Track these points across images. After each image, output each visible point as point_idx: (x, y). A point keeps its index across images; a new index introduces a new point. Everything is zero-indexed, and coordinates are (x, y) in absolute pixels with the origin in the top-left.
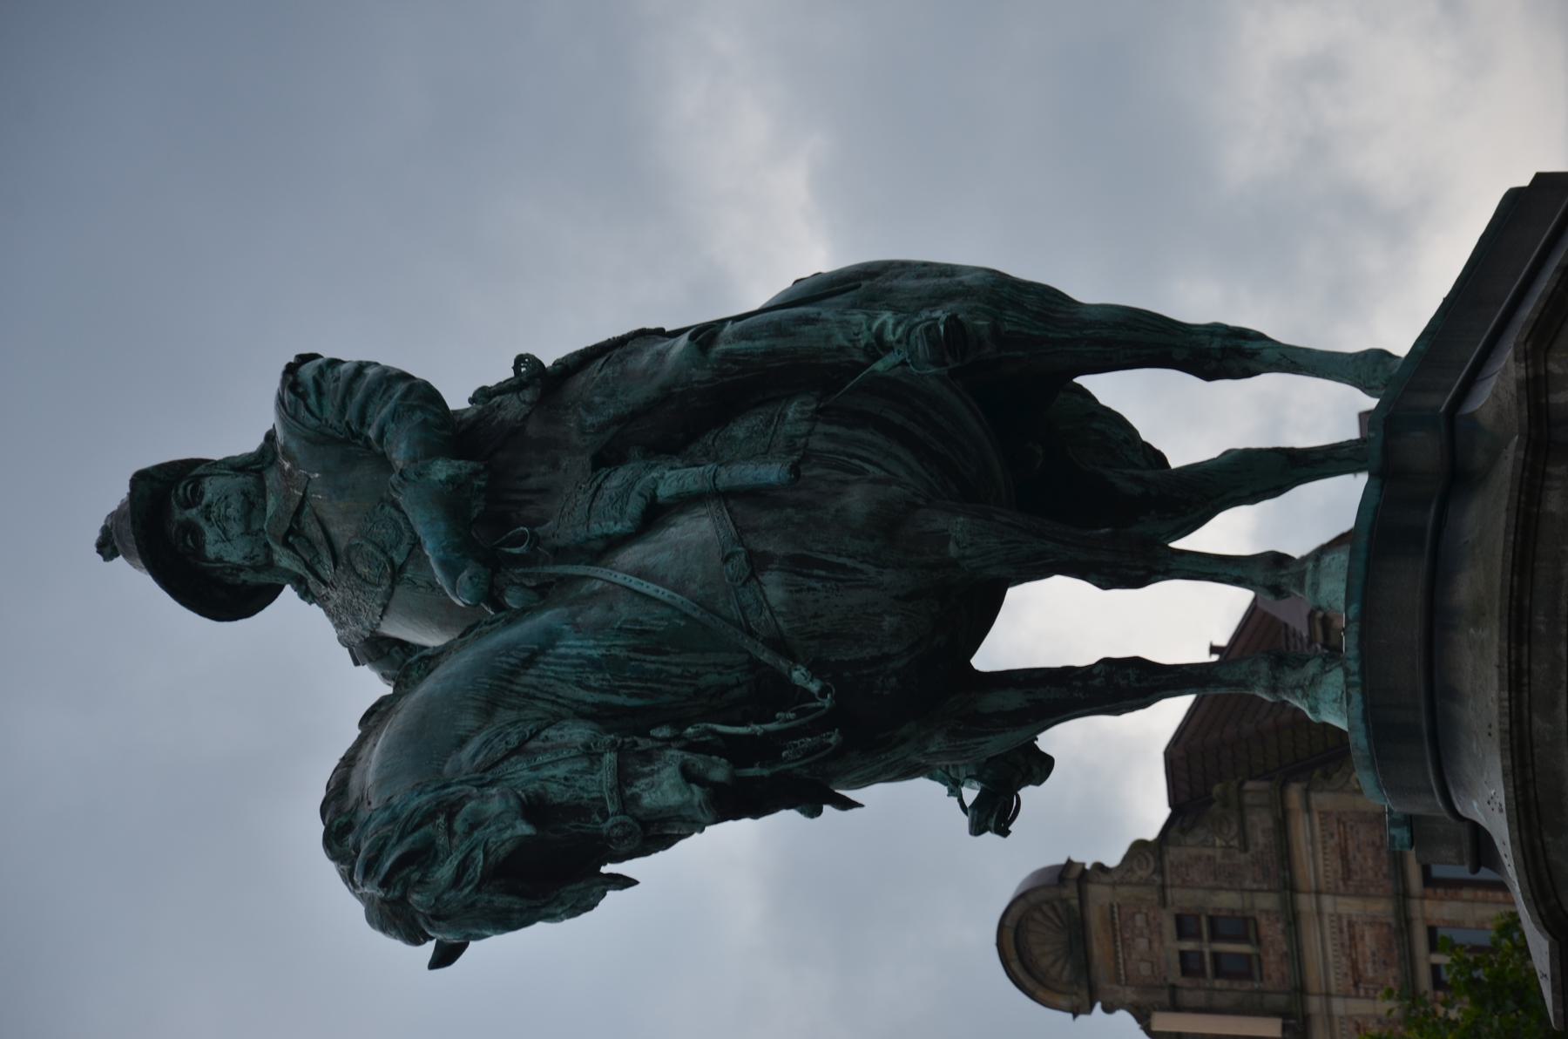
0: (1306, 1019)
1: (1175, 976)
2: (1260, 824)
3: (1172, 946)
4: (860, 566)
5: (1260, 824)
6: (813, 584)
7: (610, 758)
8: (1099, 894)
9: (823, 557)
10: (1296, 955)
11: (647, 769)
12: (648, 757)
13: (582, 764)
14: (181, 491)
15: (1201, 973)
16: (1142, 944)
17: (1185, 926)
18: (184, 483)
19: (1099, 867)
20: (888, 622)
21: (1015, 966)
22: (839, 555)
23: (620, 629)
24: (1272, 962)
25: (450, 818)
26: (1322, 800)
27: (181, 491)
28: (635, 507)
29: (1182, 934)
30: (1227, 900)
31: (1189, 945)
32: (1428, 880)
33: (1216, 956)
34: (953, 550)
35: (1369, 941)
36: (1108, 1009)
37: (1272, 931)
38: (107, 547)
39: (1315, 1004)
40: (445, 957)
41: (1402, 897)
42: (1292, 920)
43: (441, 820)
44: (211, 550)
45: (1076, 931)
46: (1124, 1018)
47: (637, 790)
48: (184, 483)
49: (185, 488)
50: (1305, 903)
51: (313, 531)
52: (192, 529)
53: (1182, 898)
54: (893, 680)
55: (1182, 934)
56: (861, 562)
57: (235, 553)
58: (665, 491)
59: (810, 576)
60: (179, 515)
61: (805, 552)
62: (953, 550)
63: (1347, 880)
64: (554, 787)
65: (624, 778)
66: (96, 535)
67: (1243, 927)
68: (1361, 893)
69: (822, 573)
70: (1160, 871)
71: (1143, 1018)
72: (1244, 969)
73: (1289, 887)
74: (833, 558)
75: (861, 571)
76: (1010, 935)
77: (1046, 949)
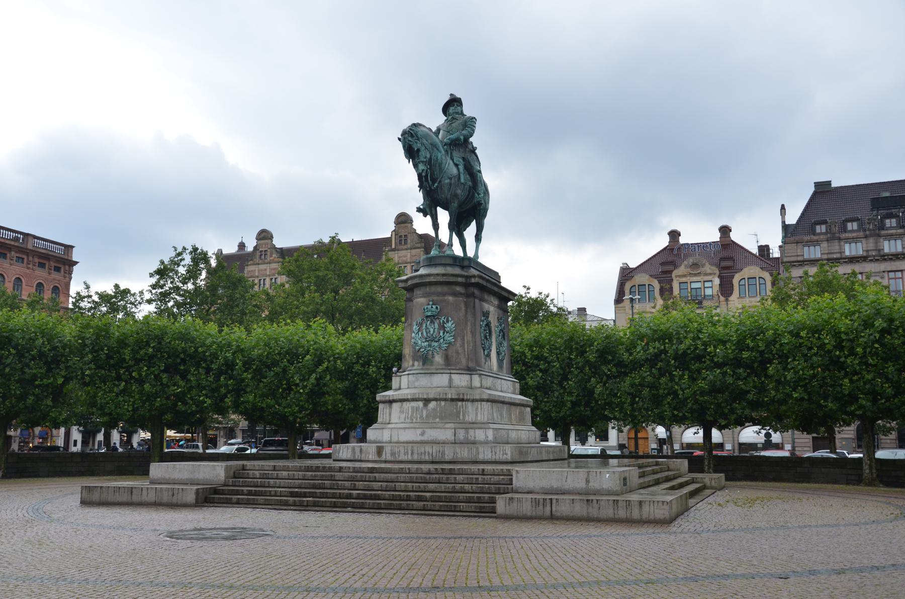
0: (395, 251)
2: (418, 245)
5: (418, 245)
8: (409, 225)
10: (402, 250)
12: (425, 165)
17: (406, 236)
24: (402, 247)
28: (458, 163)
30: (409, 241)
32: (412, 266)
35: (405, 259)
37: (405, 247)
38: (451, 95)
39: (396, 252)
40: (399, 139)
41: (410, 263)
42: (407, 249)
44: (451, 108)
45: (404, 222)
46: (394, 228)
50: (409, 251)
51: (454, 121)
52: (454, 105)
53: (409, 235)
57: (451, 111)
58: (460, 167)
60: (456, 104)
63: (412, 256)
65: (423, 162)
66: (453, 93)
67: (406, 243)
71: (394, 231)
72: (400, 243)
73: (411, 249)
77: (402, 218)
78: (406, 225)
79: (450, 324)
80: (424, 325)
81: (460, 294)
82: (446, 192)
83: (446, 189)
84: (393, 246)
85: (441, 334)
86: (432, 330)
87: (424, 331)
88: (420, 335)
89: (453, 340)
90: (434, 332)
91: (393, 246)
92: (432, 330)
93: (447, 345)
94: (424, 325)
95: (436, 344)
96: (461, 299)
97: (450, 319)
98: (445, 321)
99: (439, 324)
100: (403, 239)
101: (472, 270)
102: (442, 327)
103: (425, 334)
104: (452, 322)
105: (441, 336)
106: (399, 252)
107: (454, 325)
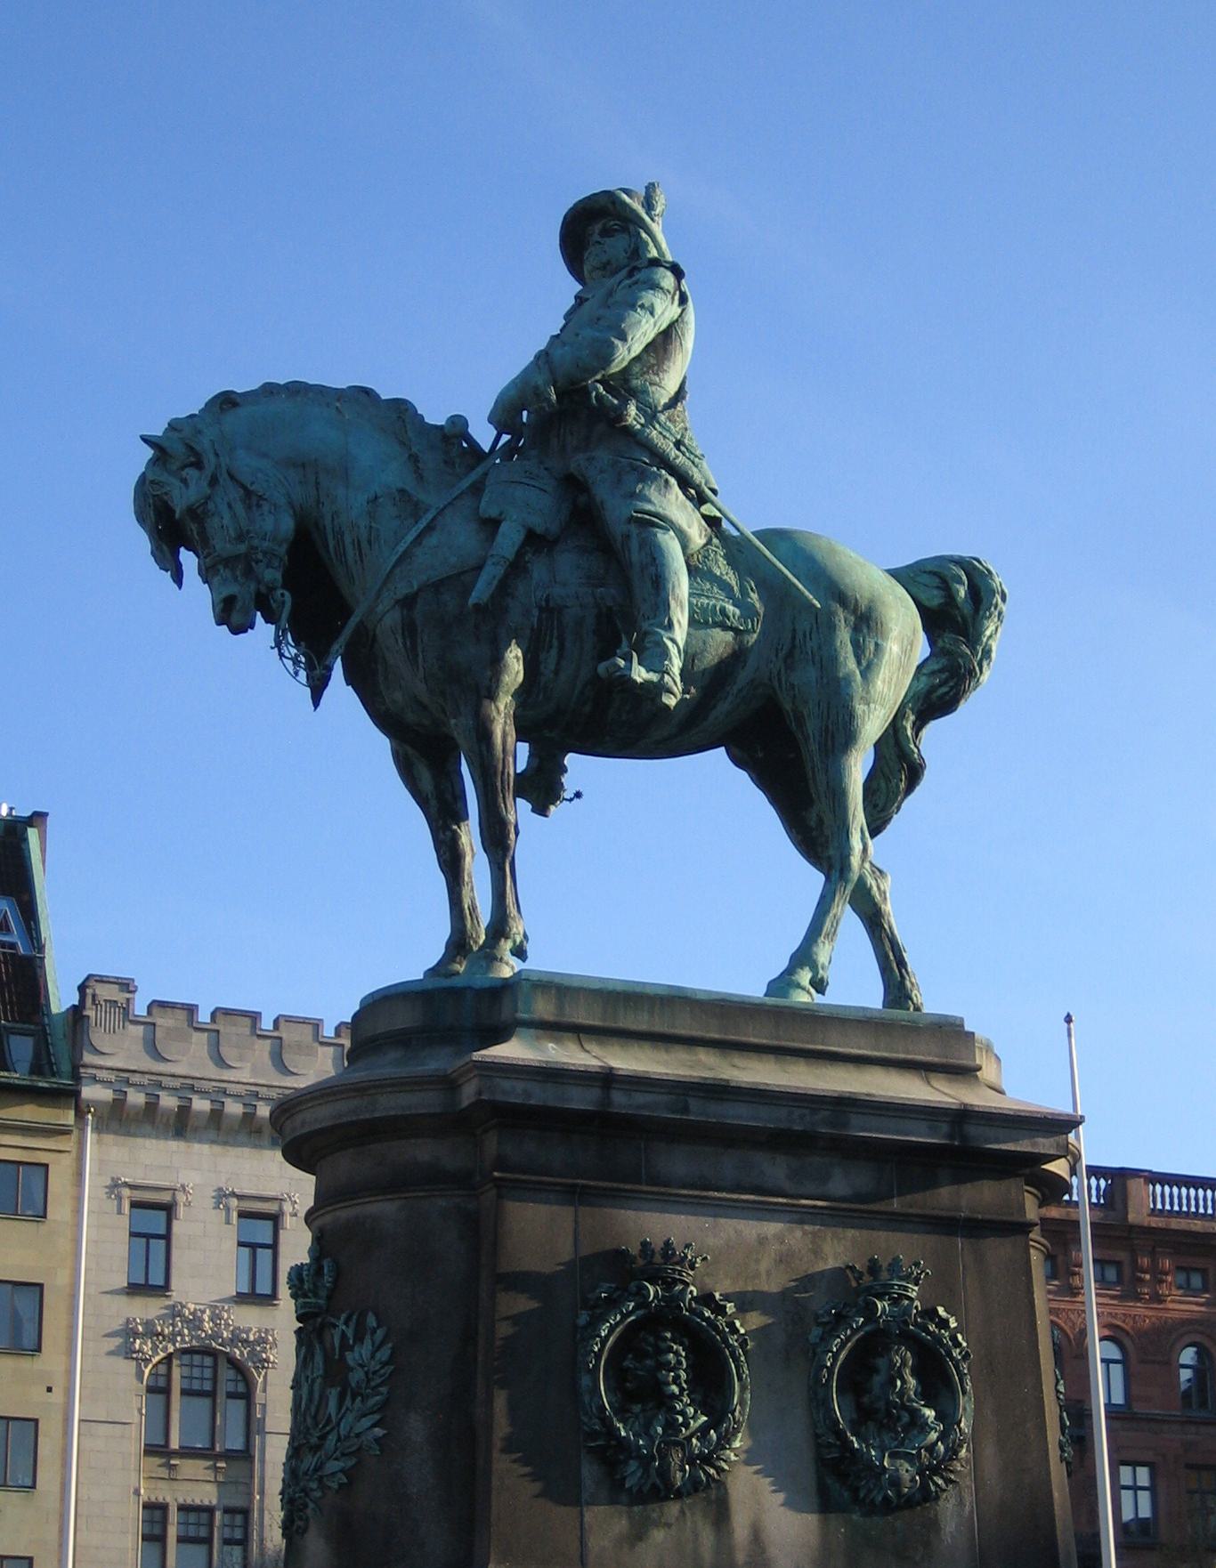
4: (420, 667)
6: (400, 641)
7: (242, 548)
9: (419, 641)
11: (238, 573)
12: (249, 572)
13: (233, 534)
14: (612, 223)
18: (617, 222)
20: (398, 696)
22: (423, 652)
23: (371, 527)
25: (191, 465)
27: (612, 223)
34: (453, 721)
43: (192, 459)
47: (222, 571)
48: (617, 222)
49: (616, 225)
54: (383, 708)
56: (423, 667)
59: (404, 638)
61: (419, 629)
62: (453, 721)
64: (216, 520)
69: (408, 643)
74: (419, 649)
75: (418, 668)
79: (365, 1349)
81: (434, 1178)
89: (378, 1432)
93: (351, 1462)
96: (442, 1203)
97: (371, 1321)
98: (350, 1333)
104: (380, 1334)
105: (329, 1420)
107: (384, 1354)
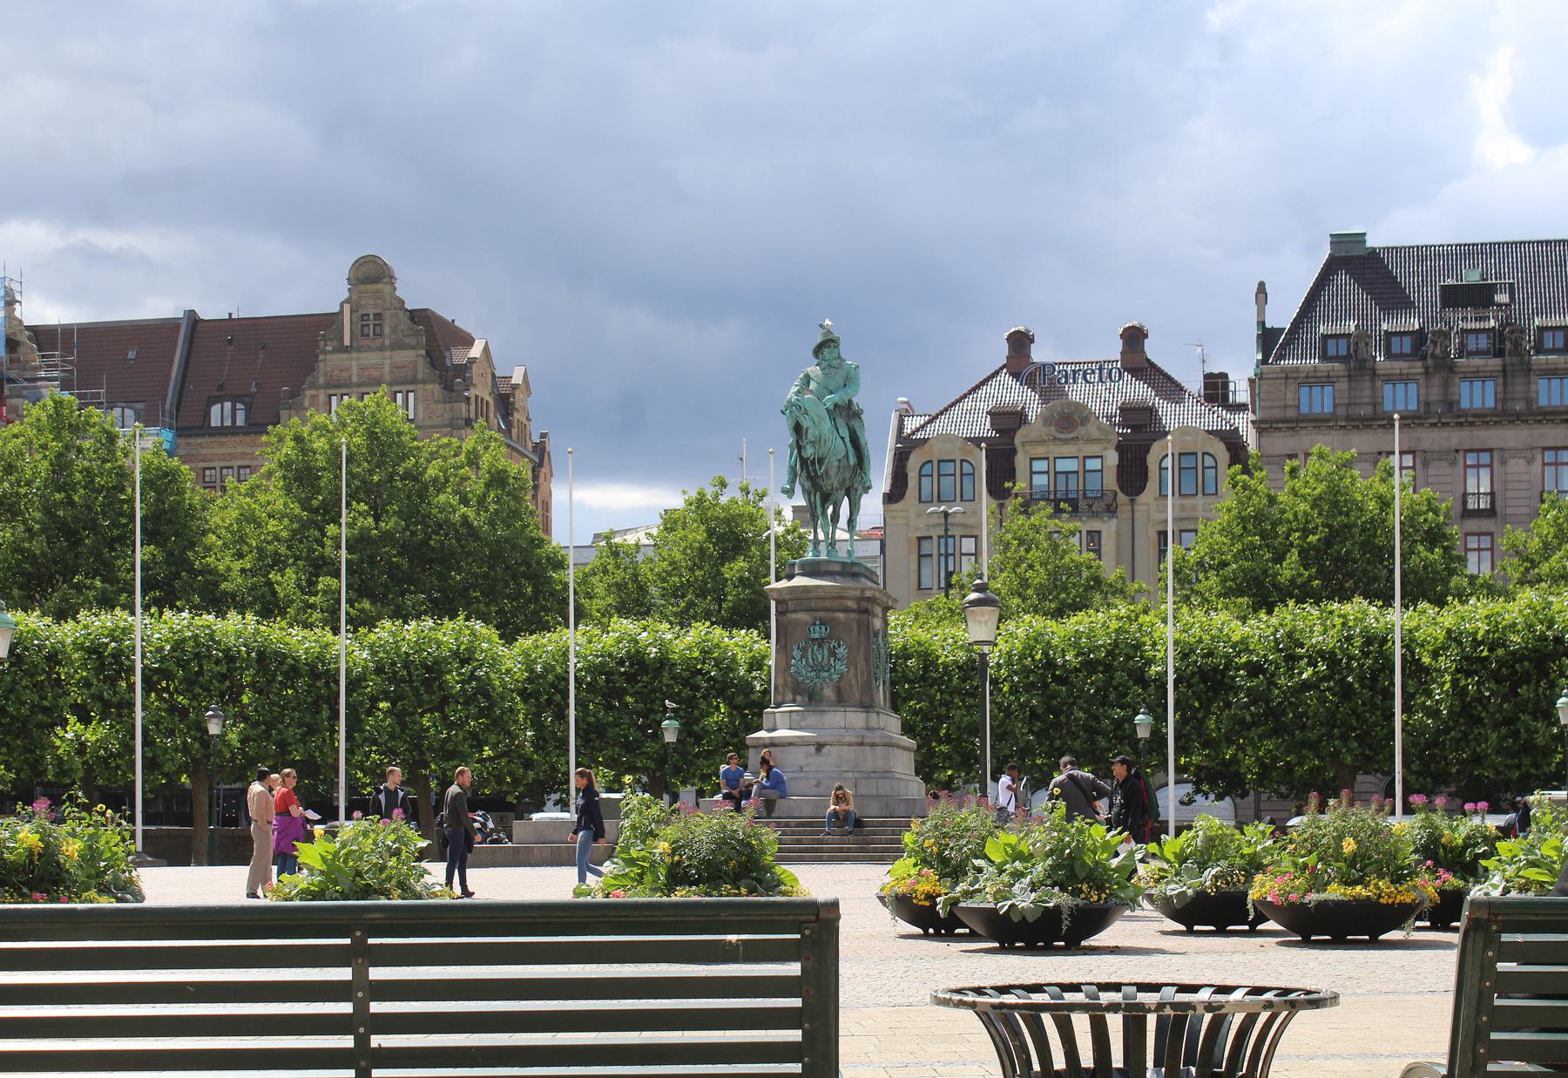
1: (361, 312)
2: (412, 341)
3: (371, 312)
5: (412, 341)
8: (387, 288)
10: (369, 349)
15: (363, 320)
16: (371, 302)
17: (378, 316)
19: (395, 289)
21: (362, 260)
26: (421, 361)
29: (374, 315)
30: (387, 330)
31: (371, 316)
33: (368, 325)
36: (349, 289)
37: (378, 342)
39: (354, 355)
42: (381, 349)
45: (376, 280)
46: (347, 295)
50: (387, 354)
53: (387, 315)
55: (374, 315)
68: (392, 372)
70: (396, 308)
71: (346, 301)
76: (373, 259)
78: (379, 286)
80: (810, 650)
82: (833, 476)
83: (833, 473)
84: (347, 342)
85: (832, 662)
86: (820, 657)
87: (810, 657)
88: (804, 663)
90: (823, 659)
91: (347, 342)
92: (820, 657)
94: (810, 650)
95: (826, 674)
99: (829, 649)
100: (371, 323)
101: (863, 580)
102: (833, 653)
103: (811, 661)
106: (362, 355)
